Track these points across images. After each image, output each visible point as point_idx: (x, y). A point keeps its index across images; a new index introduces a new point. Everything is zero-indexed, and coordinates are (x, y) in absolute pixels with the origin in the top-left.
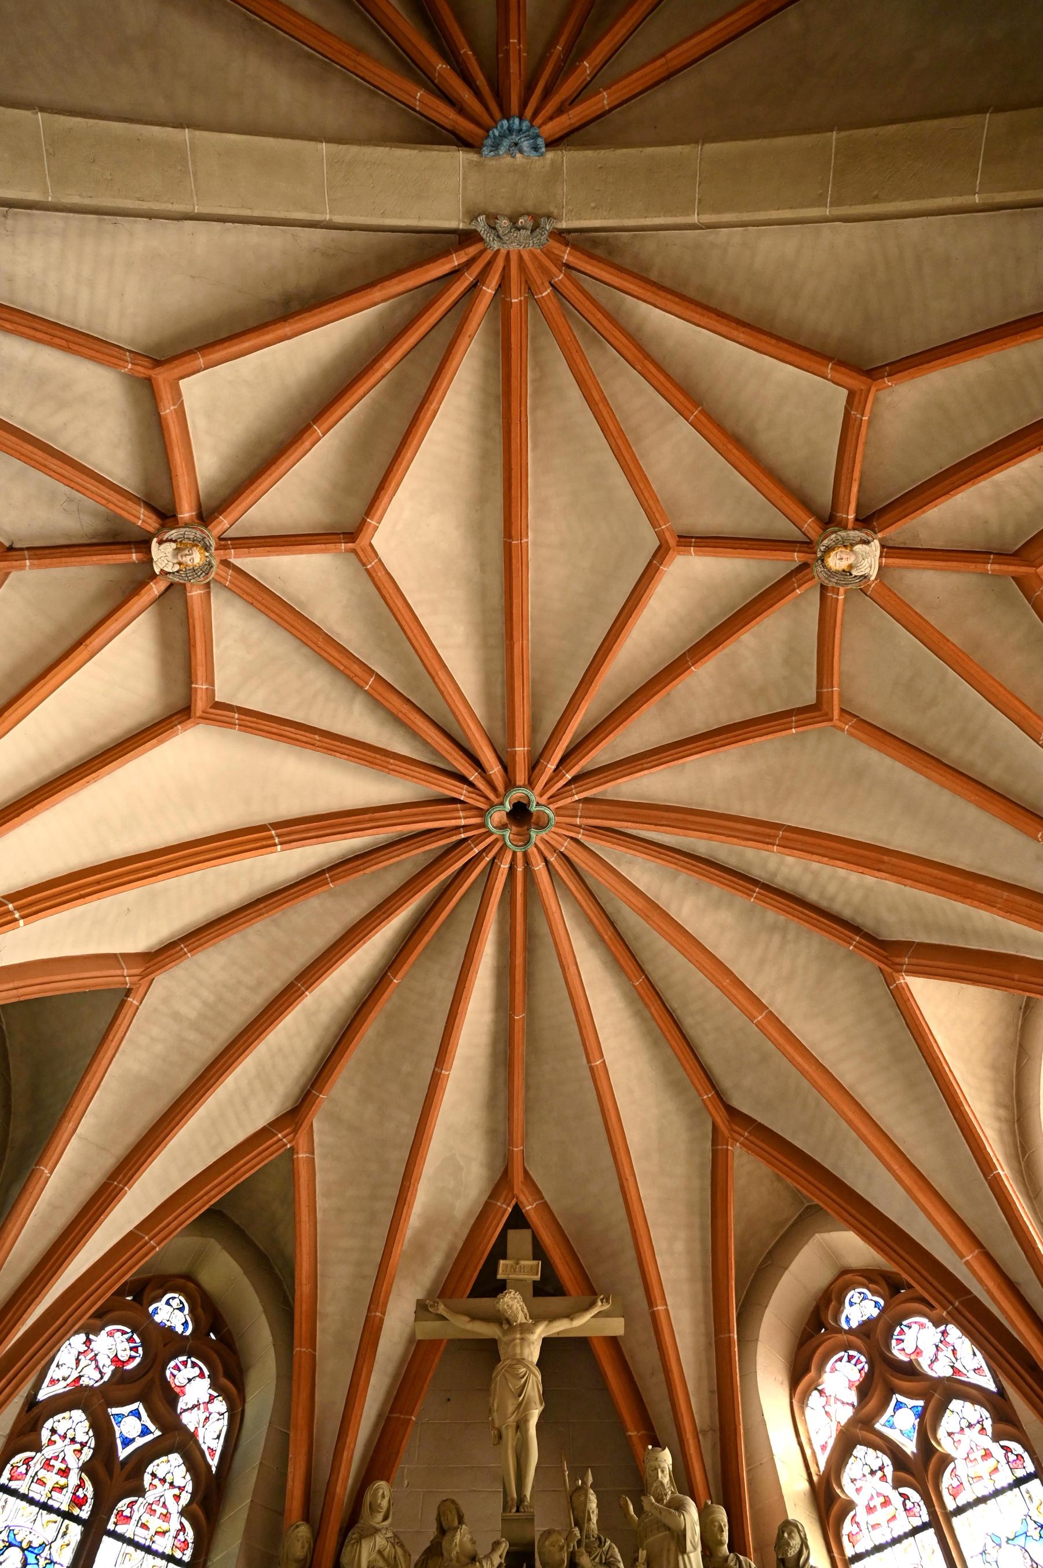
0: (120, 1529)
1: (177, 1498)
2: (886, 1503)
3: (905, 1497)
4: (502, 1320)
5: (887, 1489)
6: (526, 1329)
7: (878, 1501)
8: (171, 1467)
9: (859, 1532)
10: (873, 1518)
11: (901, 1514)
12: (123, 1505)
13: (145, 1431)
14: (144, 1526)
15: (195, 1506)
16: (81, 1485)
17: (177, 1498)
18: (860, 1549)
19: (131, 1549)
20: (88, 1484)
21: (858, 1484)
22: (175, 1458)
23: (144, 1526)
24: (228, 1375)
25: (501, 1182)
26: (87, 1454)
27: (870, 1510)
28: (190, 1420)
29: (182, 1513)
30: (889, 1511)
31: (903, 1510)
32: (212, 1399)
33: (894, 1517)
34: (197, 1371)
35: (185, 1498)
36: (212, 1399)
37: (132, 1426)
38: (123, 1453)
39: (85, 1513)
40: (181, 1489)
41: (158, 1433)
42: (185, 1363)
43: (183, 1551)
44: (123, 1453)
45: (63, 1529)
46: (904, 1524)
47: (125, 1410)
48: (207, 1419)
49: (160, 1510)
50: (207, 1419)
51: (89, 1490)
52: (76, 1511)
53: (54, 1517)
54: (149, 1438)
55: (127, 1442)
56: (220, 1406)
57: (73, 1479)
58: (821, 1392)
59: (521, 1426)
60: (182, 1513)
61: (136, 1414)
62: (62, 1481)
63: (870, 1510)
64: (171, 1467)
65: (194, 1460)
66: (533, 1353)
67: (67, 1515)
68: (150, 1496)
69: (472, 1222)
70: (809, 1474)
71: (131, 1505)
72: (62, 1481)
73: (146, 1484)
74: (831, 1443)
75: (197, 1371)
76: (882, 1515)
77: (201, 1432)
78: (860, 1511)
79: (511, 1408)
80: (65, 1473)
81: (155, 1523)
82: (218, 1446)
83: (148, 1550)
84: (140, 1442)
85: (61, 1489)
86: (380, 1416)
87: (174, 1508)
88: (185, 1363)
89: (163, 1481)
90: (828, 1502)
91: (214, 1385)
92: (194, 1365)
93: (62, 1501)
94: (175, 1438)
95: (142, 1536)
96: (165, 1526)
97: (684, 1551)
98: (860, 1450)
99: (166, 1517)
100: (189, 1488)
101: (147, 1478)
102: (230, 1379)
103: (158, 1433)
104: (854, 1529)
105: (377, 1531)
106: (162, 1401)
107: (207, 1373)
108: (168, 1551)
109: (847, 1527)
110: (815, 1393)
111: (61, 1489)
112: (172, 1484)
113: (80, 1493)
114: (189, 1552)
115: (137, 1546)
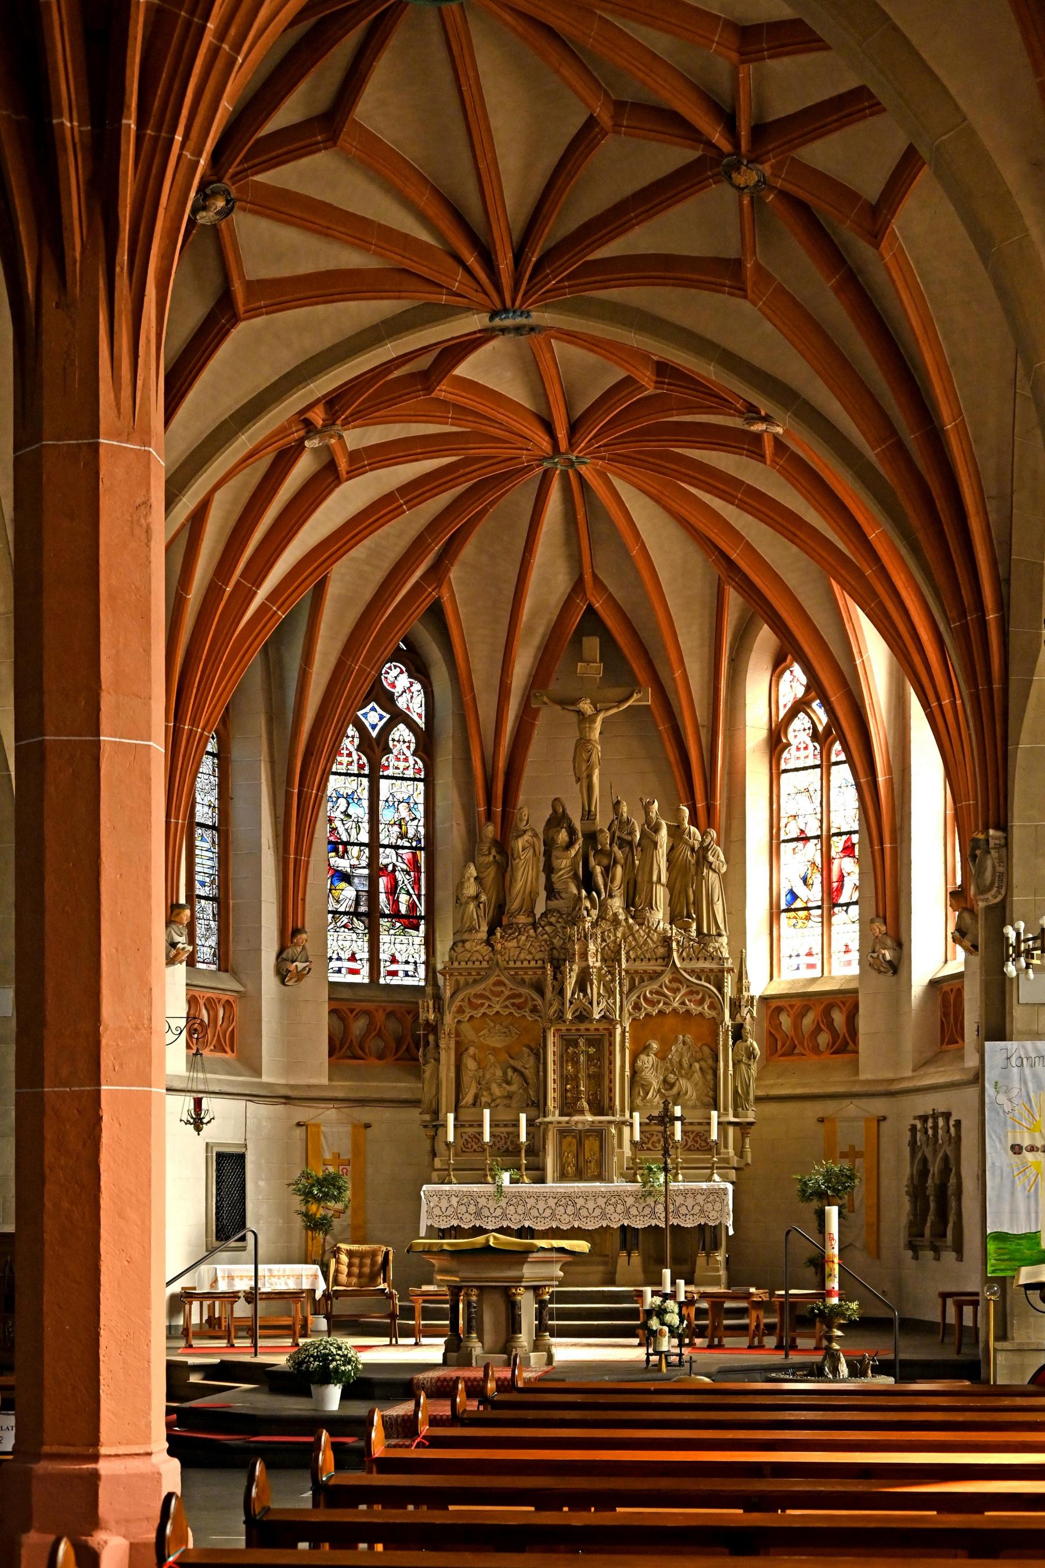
0: (386, 773)
1: (408, 747)
2: (806, 748)
3: (816, 748)
4: (579, 713)
5: (808, 740)
6: (592, 719)
7: (802, 746)
8: (401, 731)
9: (790, 759)
10: (798, 754)
11: (811, 756)
12: (383, 761)
13: (381, 717)
14: (397, 768)
15: (420, 753)
16: (360, 758)
17: (408, 747)
18: (788, 767)
19: (394, 781)
20: (363, 757)
21: (796, 733)
22: (402, 726)
23: (397, 768)
24: (418, 671)
25: (578, 586)
26: (357, 741)
27: (798, 749)
28: (401, 703)
29: (413, 755)
30: (806, 753)
31: (811, 755)
32: (411, 684)
33: (807, 757)
34: (398, 670)
35: (413, 746)
36: (411, 684)
37: (373, 717)
38: (374, 734)
39: (366, 771)
40: (409, 742)
41: (388, 716)
42: (390, 668)
43: (419, 773)
44: (374, 734)
46: (811, 762)
47: (367, 709)
48: (412, 697)
49: (402, 757)
50: (412, 697)
51: (364, 760)
52: (362, 772)
53: (353, 778)
54: (384, 720)
55: (374, 727)
56: (417, 686)
57: (355, 757)
58: (791, 672)
59: (590, 777)
60: (413, 755)
61: (373, 709)
62: (350, 759)
63: (798, 749)
64: (401, 731)
65: (411, 725)
66: (596, 735)
67: (358, 775)
68: (395, 751)
69: (562, 604)
70: (771, 725)
71: (387, 760)
72: (350, 759)
73: (391, 746)
74: (789, 705)
75: (398, 670)
76: (802, 753)
77: (410, 705)
78: (793, 748)
79: (584, 768)
80: (350, 755)
81: (402, 765)
82: (422, 711)
83: (403, 779)
84: (381, 724)
85: (350, 763)
86: (516, 717)
87: (408, 753)
88: (390, 668)
89: (399, 741)
90: (776, 742)
91: (410, 676)
92: (396, 667)
93: (354, 769)
94: (398, 717)
95: (397, 773)
96: (407, 764)
97: (656, 848)
98: (802, 715)
99: (406, 760)
100: (413, 740)
101: (391, 743)
102: (419, 671)
103: (388, 716)
104: (788, 756)
105: (525, 832)
106: (386, 700)
107: (404, 669)
108: (412, 776)
109: (785, 754)
110: (788, 672)
111: (350, 763)
112: (404, 742)
113: (361, 762)
114: (423, 773)
115: (397, 778)
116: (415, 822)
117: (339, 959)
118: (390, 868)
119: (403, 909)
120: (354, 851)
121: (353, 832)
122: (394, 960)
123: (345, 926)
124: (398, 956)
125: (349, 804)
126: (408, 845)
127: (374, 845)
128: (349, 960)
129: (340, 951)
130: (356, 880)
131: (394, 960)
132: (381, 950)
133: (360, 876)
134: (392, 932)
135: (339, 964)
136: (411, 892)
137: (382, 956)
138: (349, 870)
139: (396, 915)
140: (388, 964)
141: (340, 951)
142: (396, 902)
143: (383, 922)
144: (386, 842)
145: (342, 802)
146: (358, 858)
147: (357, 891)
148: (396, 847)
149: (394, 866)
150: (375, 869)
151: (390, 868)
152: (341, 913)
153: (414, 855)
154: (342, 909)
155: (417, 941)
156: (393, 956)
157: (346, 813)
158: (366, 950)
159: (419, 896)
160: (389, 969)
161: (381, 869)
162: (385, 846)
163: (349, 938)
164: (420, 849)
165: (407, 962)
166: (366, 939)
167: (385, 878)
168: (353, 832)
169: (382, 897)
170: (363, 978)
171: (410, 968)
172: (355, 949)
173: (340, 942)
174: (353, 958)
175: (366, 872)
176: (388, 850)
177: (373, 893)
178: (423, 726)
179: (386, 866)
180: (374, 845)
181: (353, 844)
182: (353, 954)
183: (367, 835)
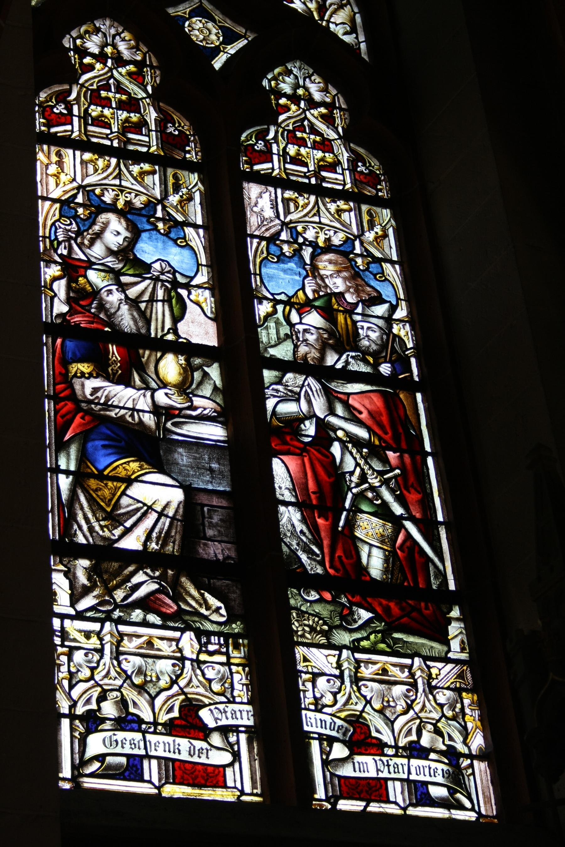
14: (297, 160)
26: (151, 79)
45: (171, 181)
116: (380, 310)
117: (127, 721)
118: (310, 428)
119: (375, 563)
120: (170, 367)
121: (161, 312)
122: (361, 741)
123: (146, 604)
124: (375, 722)
125: (136, 234)
126: (363, 368)
127: (239, 352)
128: (172, 728)
129: (130, 694)
130: (183, 457)
131: (361, 741)
132: (308, 699)
133: (196, 445)
134: (344, 638)
135: (129, 741)
136: (398, 510)
137: (312, 722)
138: (149, 420)
139: (346, 580)
140: (339, 751)
141: (130, 694)
142: (347, 541)
143: (308, 603)
144: (283, 352)
145: (115, 231)
146: (184, 388)
147: (188, 490)
148: (323, 374)
149: (322, 425)
150: (255, 438)
151: (310, 429)
152: (129, 556)
153: (390, 401)
154: (132, 542)
155: (445, 673)
156: (357, 722)
157: (126, 253)
158: (241, 692)
159: (428, 528)
160: (347, 771)
161: (277, 432)
162: (282, 366)
163: (166, 648)
164: (411, 387)
165: (416, 751)
166: (237, 656)
167: (292, 462)
168: (161, 312)
169: (290, 517)
170: (242, 782)
171: (431, 771)
172: (197, 690)
173: (131, 664)
174: (188, 722)
175: (215, 432)
176: (292, 379)
177: (253, 500)
178: (367, 60)
179: (294, 423)
180: (239, 352)
181: (163, 347)
182: (191, 708)
183: (212, 327)
